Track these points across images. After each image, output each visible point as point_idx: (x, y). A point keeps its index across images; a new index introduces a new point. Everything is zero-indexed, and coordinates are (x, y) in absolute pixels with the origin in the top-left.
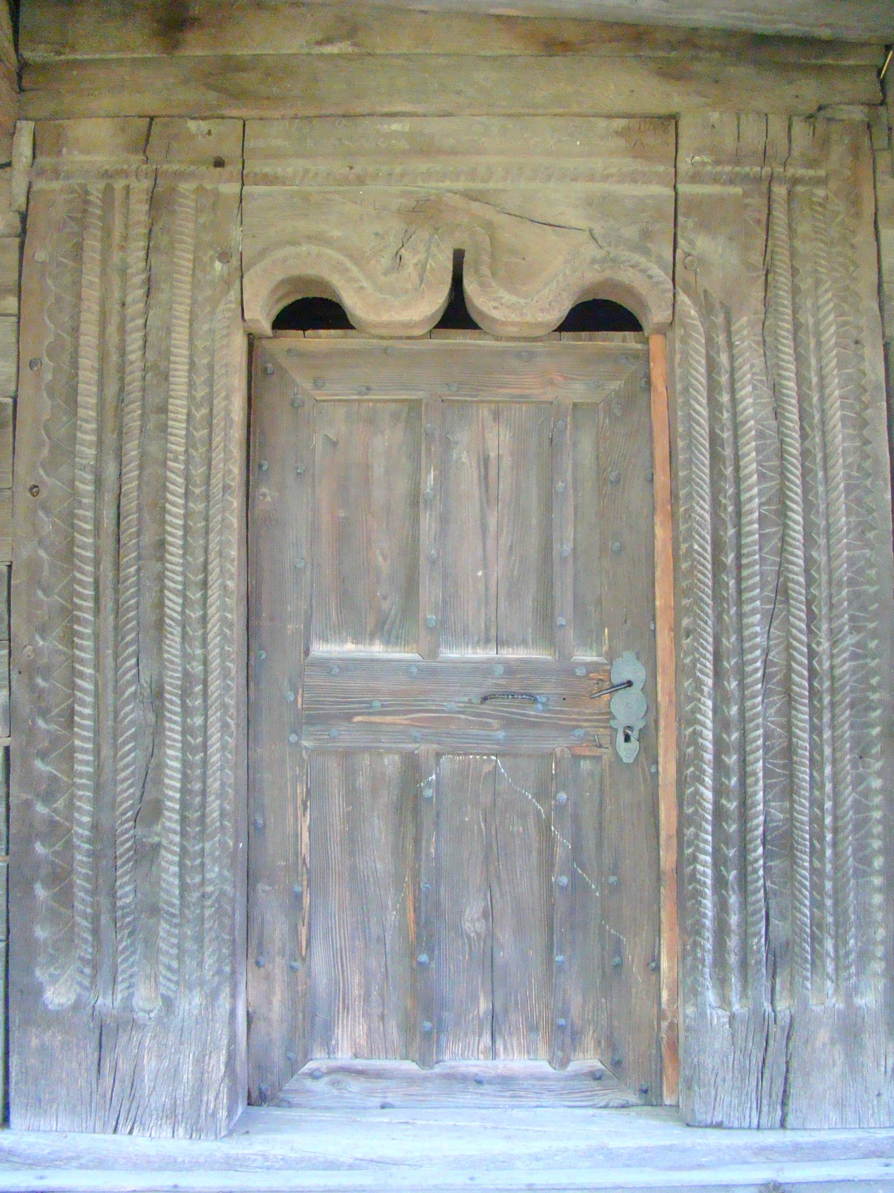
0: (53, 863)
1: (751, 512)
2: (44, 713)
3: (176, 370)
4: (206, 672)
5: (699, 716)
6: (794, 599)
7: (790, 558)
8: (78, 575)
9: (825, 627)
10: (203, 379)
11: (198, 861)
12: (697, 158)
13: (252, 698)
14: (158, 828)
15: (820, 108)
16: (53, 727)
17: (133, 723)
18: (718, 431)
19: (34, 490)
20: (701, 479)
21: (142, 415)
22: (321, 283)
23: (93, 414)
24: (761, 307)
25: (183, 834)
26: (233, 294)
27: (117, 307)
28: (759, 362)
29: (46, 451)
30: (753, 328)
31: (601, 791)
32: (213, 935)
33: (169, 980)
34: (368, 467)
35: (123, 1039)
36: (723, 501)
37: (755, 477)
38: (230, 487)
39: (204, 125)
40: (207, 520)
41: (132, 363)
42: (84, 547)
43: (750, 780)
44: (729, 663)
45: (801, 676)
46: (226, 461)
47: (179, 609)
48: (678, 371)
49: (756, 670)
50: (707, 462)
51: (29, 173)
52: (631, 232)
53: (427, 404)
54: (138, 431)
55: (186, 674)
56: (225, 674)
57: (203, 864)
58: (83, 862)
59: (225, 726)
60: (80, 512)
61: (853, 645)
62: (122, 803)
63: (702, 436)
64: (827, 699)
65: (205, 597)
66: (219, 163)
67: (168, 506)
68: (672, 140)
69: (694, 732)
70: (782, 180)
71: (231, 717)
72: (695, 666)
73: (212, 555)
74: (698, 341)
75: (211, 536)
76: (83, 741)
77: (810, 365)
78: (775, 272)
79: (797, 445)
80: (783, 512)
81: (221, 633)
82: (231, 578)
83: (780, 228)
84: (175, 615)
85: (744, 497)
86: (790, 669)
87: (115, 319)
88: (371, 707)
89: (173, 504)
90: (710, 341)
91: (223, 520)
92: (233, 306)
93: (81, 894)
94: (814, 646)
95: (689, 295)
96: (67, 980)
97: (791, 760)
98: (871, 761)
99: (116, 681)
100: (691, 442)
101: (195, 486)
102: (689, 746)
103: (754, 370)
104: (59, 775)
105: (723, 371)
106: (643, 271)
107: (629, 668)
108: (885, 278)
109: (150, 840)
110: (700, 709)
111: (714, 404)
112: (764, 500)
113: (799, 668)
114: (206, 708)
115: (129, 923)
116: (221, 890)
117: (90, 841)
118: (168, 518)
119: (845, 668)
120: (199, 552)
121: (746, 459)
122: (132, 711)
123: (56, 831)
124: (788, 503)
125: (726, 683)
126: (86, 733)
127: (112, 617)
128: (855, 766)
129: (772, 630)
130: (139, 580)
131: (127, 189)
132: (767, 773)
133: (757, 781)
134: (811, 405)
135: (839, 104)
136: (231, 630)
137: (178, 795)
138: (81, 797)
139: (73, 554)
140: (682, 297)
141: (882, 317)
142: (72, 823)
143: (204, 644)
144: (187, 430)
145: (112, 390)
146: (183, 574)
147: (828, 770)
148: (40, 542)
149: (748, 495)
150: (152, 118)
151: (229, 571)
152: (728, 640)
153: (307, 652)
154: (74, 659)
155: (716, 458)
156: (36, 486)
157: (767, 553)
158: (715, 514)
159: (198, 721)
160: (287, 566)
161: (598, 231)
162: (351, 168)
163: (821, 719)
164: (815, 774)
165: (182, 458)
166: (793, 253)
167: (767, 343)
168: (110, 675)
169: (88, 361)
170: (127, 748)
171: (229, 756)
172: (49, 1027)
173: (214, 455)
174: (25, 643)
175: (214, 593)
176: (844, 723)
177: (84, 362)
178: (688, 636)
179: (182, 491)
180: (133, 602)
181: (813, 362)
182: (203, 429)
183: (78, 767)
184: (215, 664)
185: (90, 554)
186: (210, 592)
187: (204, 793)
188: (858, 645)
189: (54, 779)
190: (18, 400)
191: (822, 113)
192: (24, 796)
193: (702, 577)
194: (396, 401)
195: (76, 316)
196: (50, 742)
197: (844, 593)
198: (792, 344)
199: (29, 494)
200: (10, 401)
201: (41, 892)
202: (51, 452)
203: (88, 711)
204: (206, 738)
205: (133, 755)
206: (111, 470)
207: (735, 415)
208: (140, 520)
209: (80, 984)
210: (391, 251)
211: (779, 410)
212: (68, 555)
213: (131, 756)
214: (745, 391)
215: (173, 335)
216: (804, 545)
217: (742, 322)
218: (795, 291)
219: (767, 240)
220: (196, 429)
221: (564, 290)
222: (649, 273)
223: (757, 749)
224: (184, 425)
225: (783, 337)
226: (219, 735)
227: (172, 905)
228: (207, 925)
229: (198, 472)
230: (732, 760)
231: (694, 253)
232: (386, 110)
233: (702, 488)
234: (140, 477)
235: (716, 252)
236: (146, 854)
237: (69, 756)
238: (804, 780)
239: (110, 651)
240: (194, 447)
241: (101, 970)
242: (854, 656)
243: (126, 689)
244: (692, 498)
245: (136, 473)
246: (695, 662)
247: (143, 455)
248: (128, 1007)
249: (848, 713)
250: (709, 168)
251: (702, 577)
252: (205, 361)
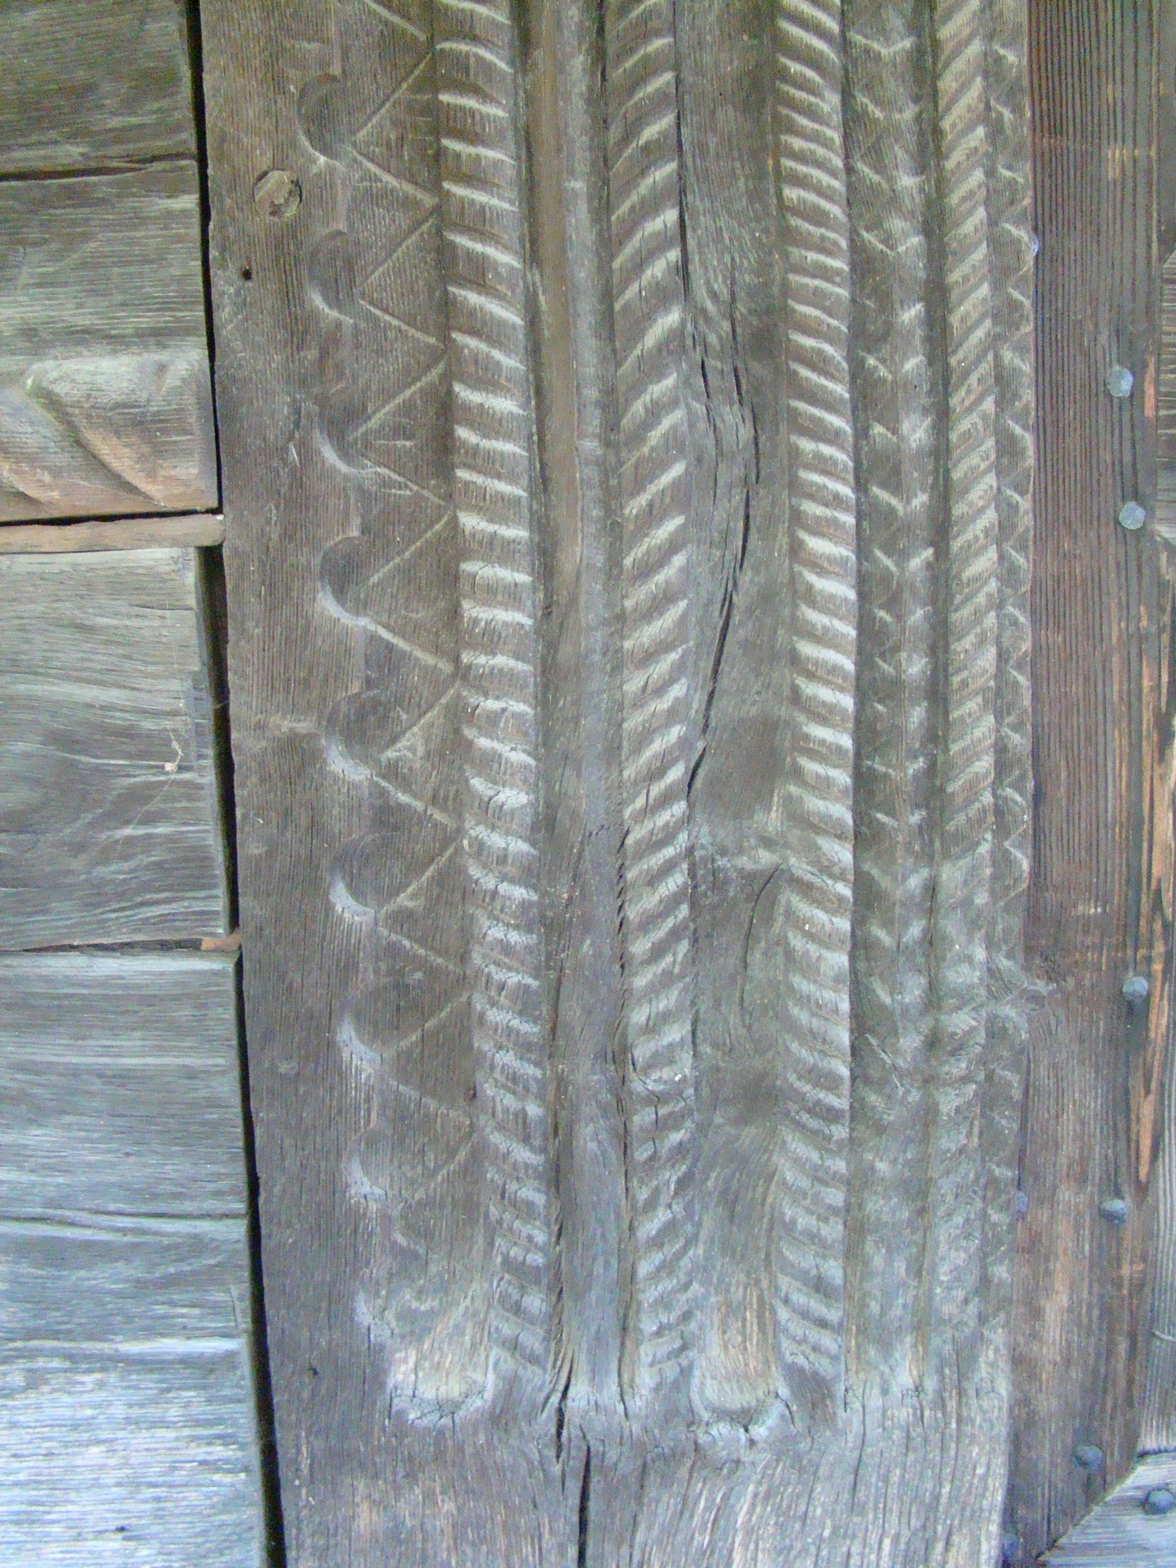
0: (393, 950)
2: (341, 422)
11: (915, 930)
14: (772, 820)
17: (674, 445)
25: (865, 837)
32: (967, 1171)
33: (822, 1324)
35: (665, 1504)
55: (864, 266)
57: (932, 941)
58: (506, 948)
62: (646, 735)
71: (1020, 418)
76: (493, 520)
93: (506, 1058)
96: (459, 1330)
99: (607, 296)
109: (744, 862)
114: (943, 381)
115: (680, 1150)
116: (992, 1020)
117: (528, 875)
123: (391, 841)
126: (503, 487)
127: (579, 63)
138: (493, 719)
142: (458, 814)
154: (445, 216)
168: (583, 273)
171: (1020, 560)
172: (411, 1476)
174: (264, 162)
187: (938, 692)
189: (385, 660)
192: (285, 724)
196: (365, 529)
201: (361, 1056)
204: (944, 493)
205: (679, 560)
209: (514, 1346)
227: (829, 1081)
228: (948, 1142)
236: (732, 911)
237: (443, 574)
239: (578, 185)
241: (578, 1287)
243: (649, 318)
248: (675, 1405)
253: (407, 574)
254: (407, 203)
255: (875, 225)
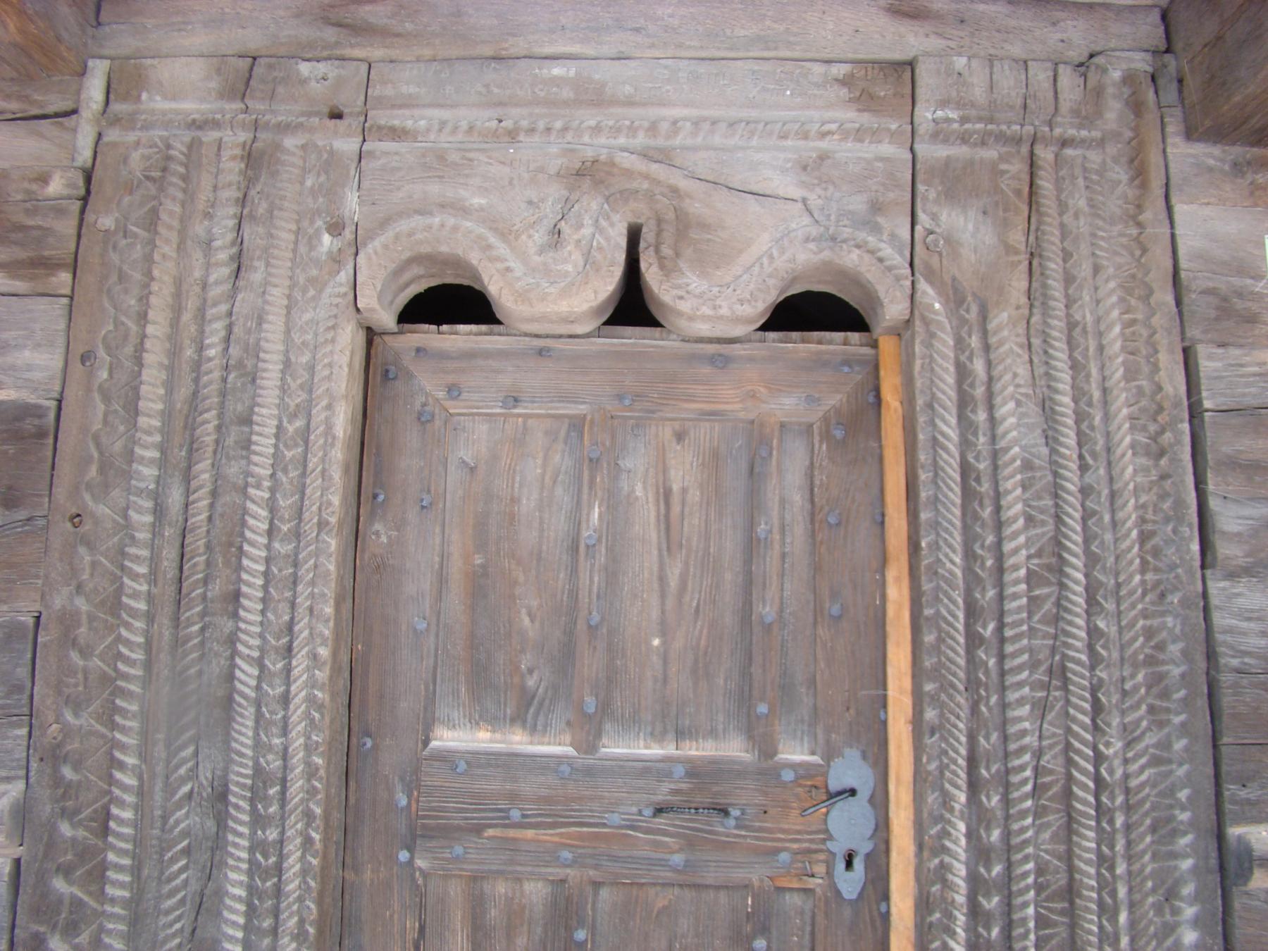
1: (1016, 568)
2: (70, 815)
3: (265, 370)
4: (285, 767)
5: (948, 843)
6: (1074, 684)
7: (1069, 628)
8: (124, 632)
9: (1115, 722)
10: (299, 381)
12: (940, 113)
13: (352, 801)
15: (1091, 56)
16: (81, 833)
17: (186, 834)
18: (972, 460)
19: (76, 519)
20: (950, 522)
21: (219, 428)
22: (457, 263)
23: (156, 423)
24: (1024, 300)
26: (344, 276)
27: (197, 289)
28: (1023, 371)
29: (93, 471)
30: (1014, 326)
31: (813, 933)
34: (514, 500)
36: (979, 552)
37: (1021, 522)
38: (328, 523)
39: (322, 68)
40: (296, 565)
41: (210, 359)
42: (135, 595)
43: (1018, 931)
44: (988, 769)
45: (1084, 787)
46: (324, 490)
47: (253, 683)
48: (918, 383)
49: (1025, 782)
50: (958, 501)
51: (98, 122)
52: (858, 204)
53: (592, 422)
54: (210, 449)
55: (258, 771)
56: (311, 772)
59: (308, 841)
60: (132, 550)
61: (1154, 746)
63: (951, 467)
64: (1119, 821)
65: (288, 670)
66: (337, 115)
67: (246, 547)
68: (908, 90)
69: (942, 862)
70: (1047, 142)
72: (942, 773)
73: (301, 611)
74: (944, 342)
75: (300, 588)
77: (1088, 376)
78: (1040, 256)
79: (1076, 479)
80: (1059, 568)
81: (307, 715)
82: (324, 643)
83: (1048, 202)
84: (247, 690)
85: (1008, 547)
86: (1070, 778)
87: (191, 304)
88: (508, 818)
89: (252, 544)
90: (960, 344)
91: (316, 566)
92: (343, 290)
94: (1101, 747)
95: (931, 283)
97: (1072, 903)
98: (1182, 905)
99: (167, 777)
100: (936, 475)
101: (282, 520)
102: (933, 883)
103: (1017, 381)
104: (86, 898)
105: (978, 383)
106: (872, 252)
107: (849, 770)
108: (1183, 263)
110: (949, 834)
111: (965, 424)
112: (1032, 551)
113: (1084, 779)
118: (245, 562)
119: (1144, 777)
120: (284, 607)
121: (1010, 498)
122: (187, 815)
124: (1066, 555)
125: (984, 799)
126: (123, 845)
128: (1159, 910)
129: (1045, 726)
130: (202, 643)
131: (220, 144)
132: (1041, 922)
133: (1027, 932)
134: (1092, 428)
135: (1113, 50)
136: (322, 715)
137: (240, 935)
139: (120, 602)
140: (923, 285)
141: (1180, 313)
143: (285, 732)
144: (276, 446)
145: (183, 392)
146: (261, 636)
147: (1123, 917)
148: (79, 588)
149: (1013, 545)
150: (255, 59)
151: (321, 634)
152: (987, 738)
153: (426, 743)
155: (968, 494)
156: (79, 515)
157: (1039, 621)
158: (968, 570)
159: (272, 835)
160: (404, 628)
161: (814, 201)
162: (500, 121)
163: (1112, 847)
164: (1105, 923)
165: (266, 484)
166: (1064, 232)
167: (1035, 345)
168: (160, 768)
169: (155, 356)
170: (176, 867)
171: (312, 884)
173: (308, 481)
175: (300, 662)
176: (1144, 852)
177: (149, 358)
178: (932, 733)
179: (266, 527)
180: (192, 671)
181: (1094, 372)
182: (296, 445)
183: (110, 891)
184: (297, 758)
185: (142, 606)
186: (294, 663)
188: (1157, 745)
190: (64, 403)
191: (1096, 60)
193: (951, 654)
194: (553, 416)
195: (144, 299)
197: (1140, 677)
198: (1065, 347)
199: (69, 525)
200: (53, 404)
202: (102, 470)
203: (127, 815)
204: (281, 857)
205: (184, 876)
206: (175, 497)
207: (993, 439)
208: (208, 564)
210: (547, 224)
211: (1050, 433)
212: (114, 605)
213: (182, 875)
214: (1005, 409)
215: (265, 326)
216: (1087, 612)
217: (1001, 318)
218: (1069, 279)
219: (1029, 218)
220: (286, 446)
221: (770, 276)
222: (880, 254)
223: (1027, 888)
224: (273, 441)
225: (1055, 339)
226: (299, 854)
229: (285, 503)
230: (992, 903)
231: (938, 230)
232: (548, 50)
233: (951, 534)
234: (212, 505)
235: (968, 230)
238: (1090, 932)
240: (285, 471)
242: (1156, 761)
243: (179, 787)
244: (939, 548)
245: (205, 502)
246: (942, 769)
247: (217, 477)
249: (1148, 839)
250: (956, 126)
251: (951, 654)
252: (305, 359)
253: (89, 873)
254: (103, 736)
255: (264, 756)
